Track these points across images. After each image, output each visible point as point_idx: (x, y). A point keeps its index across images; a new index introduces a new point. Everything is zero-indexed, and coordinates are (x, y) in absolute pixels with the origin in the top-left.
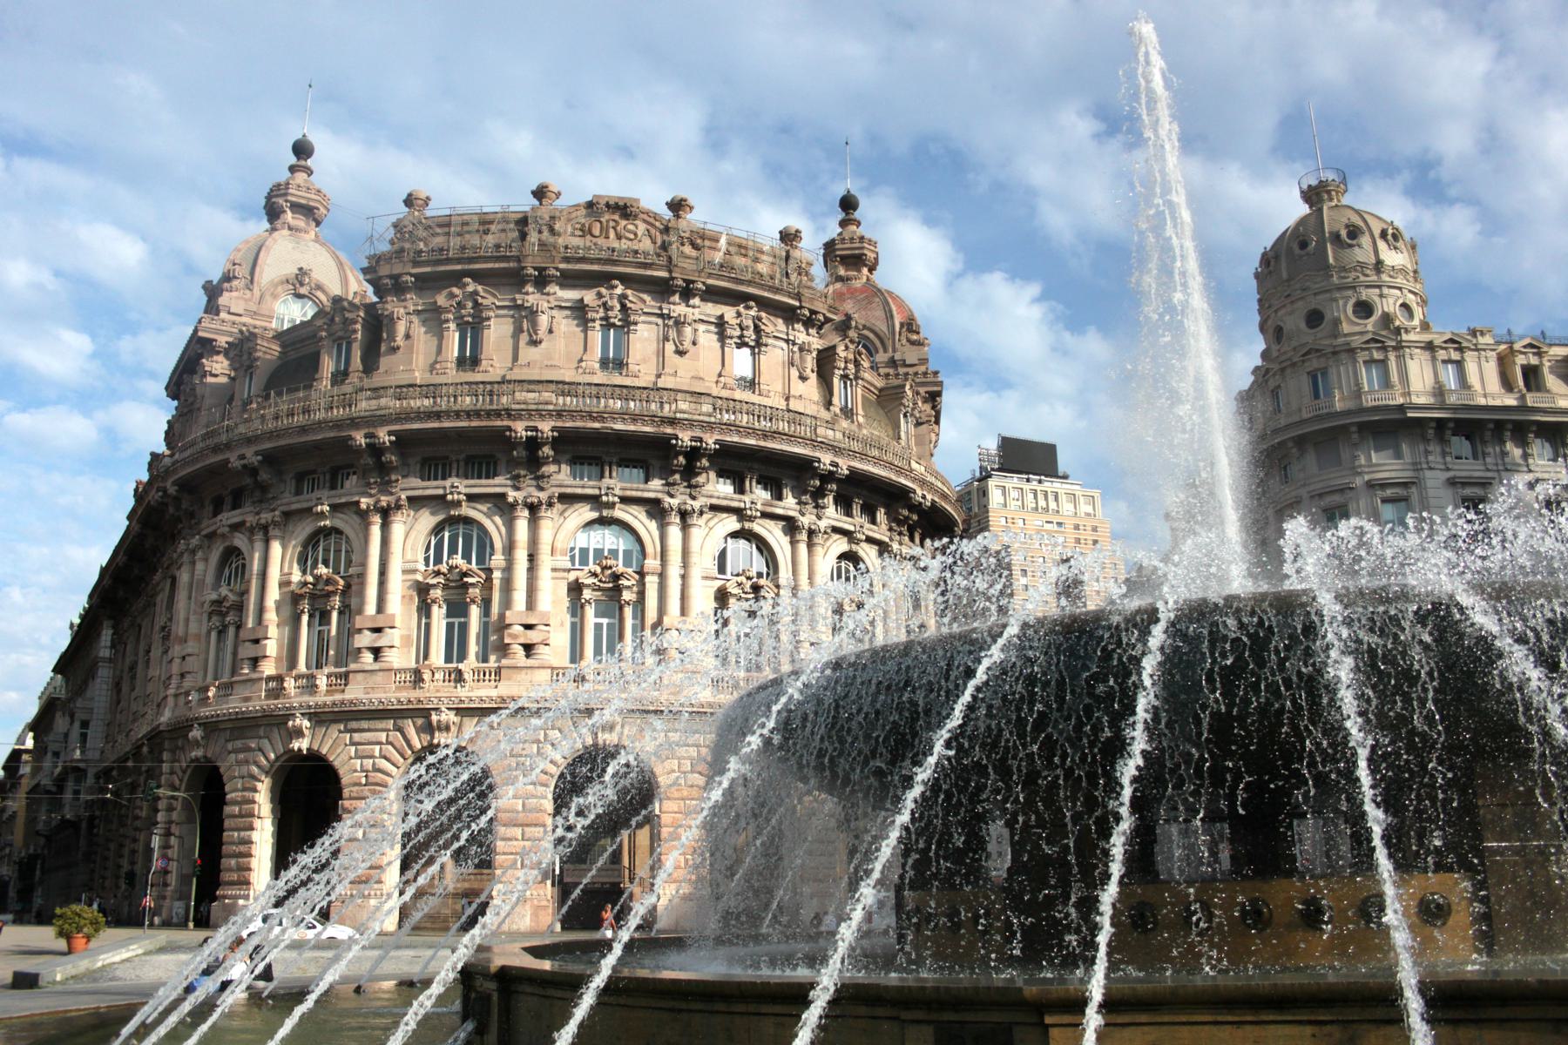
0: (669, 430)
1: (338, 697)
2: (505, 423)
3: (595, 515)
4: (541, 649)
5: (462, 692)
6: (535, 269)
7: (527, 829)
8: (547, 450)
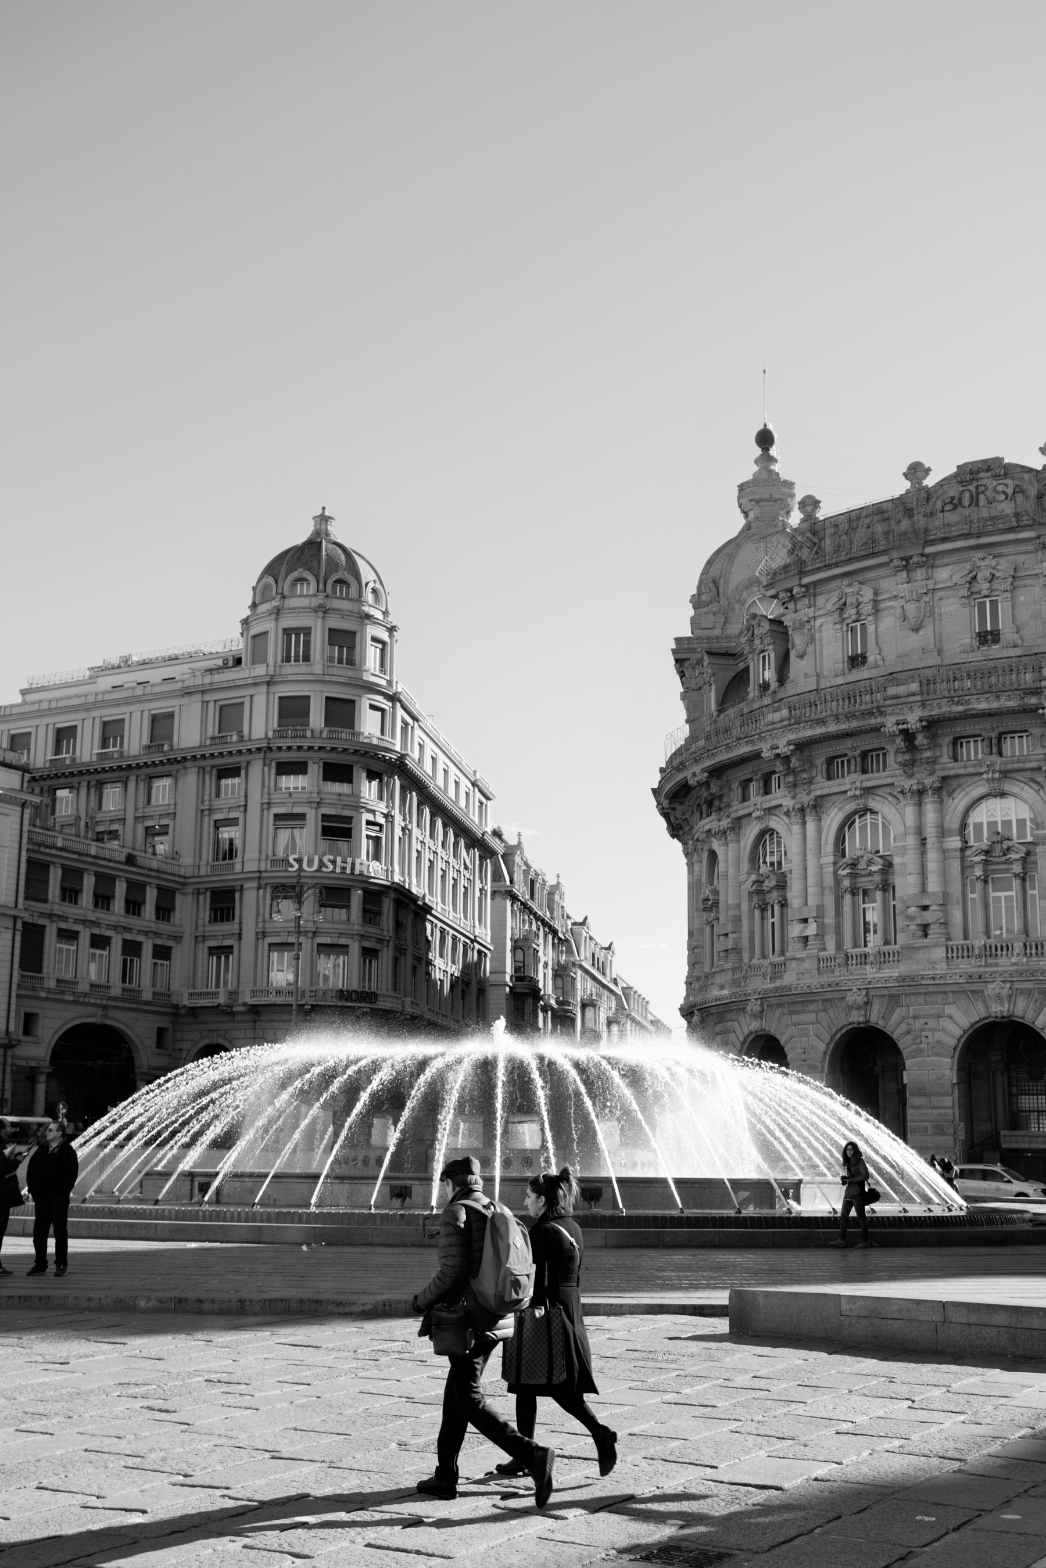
0: (1034, 701)
1: (778, 983)
2: (879, 720)
3: (981, 789)
4: (933, 930)
6: (902, 559)
7: (933, 1099)
8: (920, 740)
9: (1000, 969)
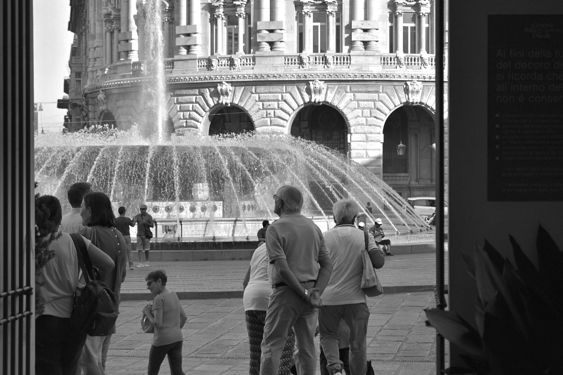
5: (234, 72)
9: (318, 72)
